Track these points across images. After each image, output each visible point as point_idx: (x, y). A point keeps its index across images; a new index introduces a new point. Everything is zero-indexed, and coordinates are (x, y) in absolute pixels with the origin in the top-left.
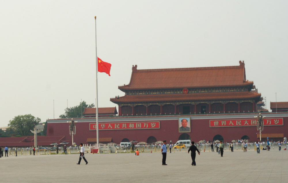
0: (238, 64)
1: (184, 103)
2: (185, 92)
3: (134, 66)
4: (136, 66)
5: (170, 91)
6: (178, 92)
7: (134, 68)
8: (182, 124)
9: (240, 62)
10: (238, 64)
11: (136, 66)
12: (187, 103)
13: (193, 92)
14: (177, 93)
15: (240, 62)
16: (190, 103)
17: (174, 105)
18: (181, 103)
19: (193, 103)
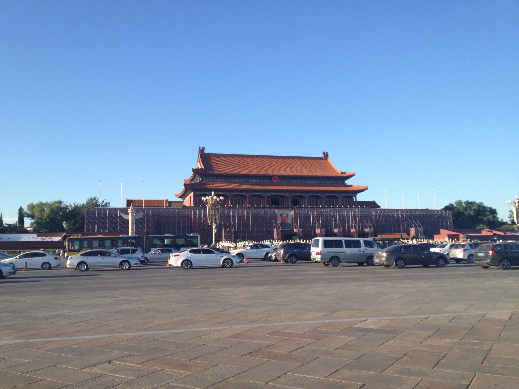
0: (322, 156)
1: (276, 194)
2: (276, 180)
3: (201, 148)
4: (204, 149)
5: (256, 179)
6: (266, 181)
7: (201, 151)
8: (281, 219)
9: (324, 153)
10: (322, 156)
11: (204, 149)
12: (280, 194)
13: (284, 181)
14: (264, 182)
15: (324, 153)
16: (283, 194)
17: (263, 195)
18: (273, 194)
19: (287, 194)
